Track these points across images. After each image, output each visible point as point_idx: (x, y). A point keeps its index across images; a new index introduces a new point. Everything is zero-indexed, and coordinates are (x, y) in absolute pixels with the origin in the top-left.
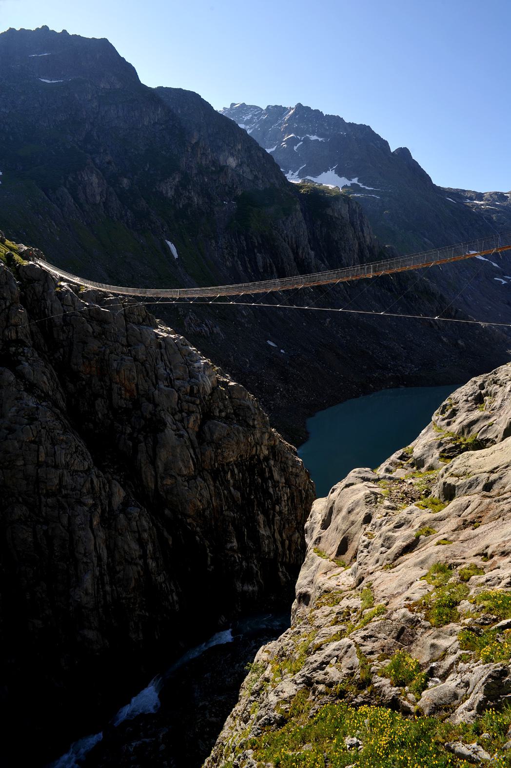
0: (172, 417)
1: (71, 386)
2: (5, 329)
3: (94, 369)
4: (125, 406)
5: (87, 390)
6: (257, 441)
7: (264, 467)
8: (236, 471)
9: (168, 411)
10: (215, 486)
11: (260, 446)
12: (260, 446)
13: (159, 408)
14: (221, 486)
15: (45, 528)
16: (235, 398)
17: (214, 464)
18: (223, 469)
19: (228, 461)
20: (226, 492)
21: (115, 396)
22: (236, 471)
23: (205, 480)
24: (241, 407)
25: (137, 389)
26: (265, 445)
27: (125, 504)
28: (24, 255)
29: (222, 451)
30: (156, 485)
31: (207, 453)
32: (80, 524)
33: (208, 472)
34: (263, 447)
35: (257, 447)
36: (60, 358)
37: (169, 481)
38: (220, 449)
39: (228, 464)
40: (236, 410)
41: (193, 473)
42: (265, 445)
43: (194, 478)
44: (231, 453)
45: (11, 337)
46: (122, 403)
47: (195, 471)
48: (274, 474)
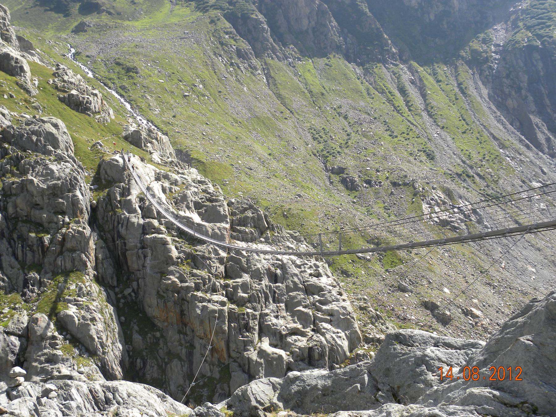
1: (137, 338)
2: (58, 256)
4: (209, 374)
28: (130, 139)
45: (65, 267)
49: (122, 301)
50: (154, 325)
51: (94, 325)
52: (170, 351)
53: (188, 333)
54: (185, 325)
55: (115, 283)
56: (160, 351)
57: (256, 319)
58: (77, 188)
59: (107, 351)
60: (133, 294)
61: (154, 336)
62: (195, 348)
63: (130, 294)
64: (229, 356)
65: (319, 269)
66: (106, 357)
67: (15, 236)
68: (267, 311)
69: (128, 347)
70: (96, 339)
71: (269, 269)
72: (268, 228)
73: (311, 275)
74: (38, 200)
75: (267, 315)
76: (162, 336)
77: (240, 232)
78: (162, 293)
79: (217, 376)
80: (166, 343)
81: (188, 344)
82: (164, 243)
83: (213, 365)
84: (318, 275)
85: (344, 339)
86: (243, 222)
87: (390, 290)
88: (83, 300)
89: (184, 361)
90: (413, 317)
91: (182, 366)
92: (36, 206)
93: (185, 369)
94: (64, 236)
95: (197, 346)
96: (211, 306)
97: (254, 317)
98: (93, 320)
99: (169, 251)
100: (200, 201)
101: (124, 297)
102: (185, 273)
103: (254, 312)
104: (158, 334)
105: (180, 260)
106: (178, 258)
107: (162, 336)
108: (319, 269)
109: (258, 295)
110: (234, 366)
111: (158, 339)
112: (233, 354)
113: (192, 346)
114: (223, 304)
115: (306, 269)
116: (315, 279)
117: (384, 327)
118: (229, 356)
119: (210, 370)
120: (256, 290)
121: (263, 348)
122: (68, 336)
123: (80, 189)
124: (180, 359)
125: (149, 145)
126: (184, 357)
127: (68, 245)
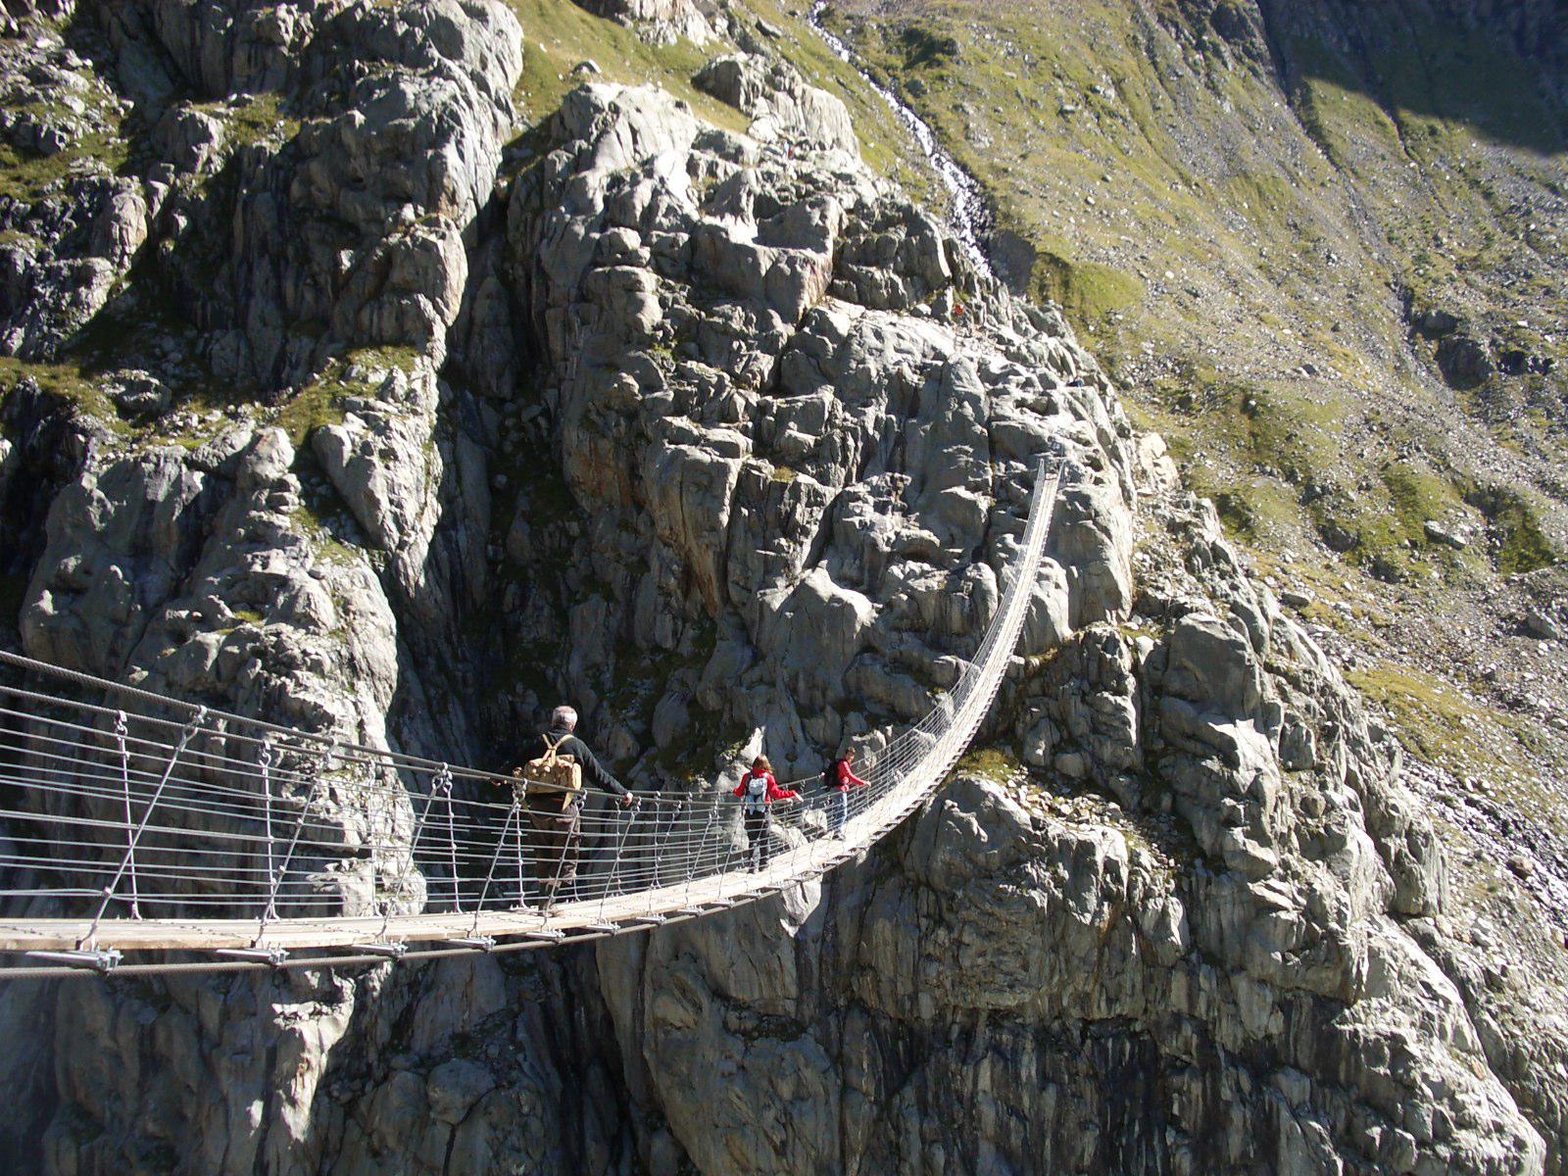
0: (795, 719)
3: (609, 474)
4: (669, 644)
5: (576, 557)
6: (1214, 944)
7: (1226, 1093)
8: (1028, 1068)
9: (793, 690)
10: (884, 1107)
11: (1225, 979)
12: (1225, 979)
13: (757, 672)
14: (924, 1113)
15: (149, 1016)
16: (1180, 696)
17: (914, 998)
18: (968, 1035)
19: (986, 1000)
20: (940, 1157)
21: (647, 597)
22: (1028, 1068)
23: (839, 1061)
24: (1190, 745)
25: (723, 573)
26: (1262, 982)
27: (463, 1043)
28: (711, 84)
29: (959, 943)
30: (639, 1013)
31: (882, 929)
32: (243, 1051)
33: (874, 1027)
34: (1242, 985)
35: (1192, 974)
36: (537, 426)
37: (674, 1011)
38: (950, 929)
39: (997, 1017)
40: (1164, 753)
41: (790, 1006)
42: (1262, 982)
43: (789, 1030)
44: (1011, 963)
45: (380, 330)
46: (664, 629)
47: (799, 1001)
48: (1284, 1154)
49: (514, 436)
50: (573, 504)
51: (387, 467)
52: (594, 572)
53: (642, 528)
54: (640, 506)
55: (507, 391)
56: (571, 572)
57: (821, 504)
58: (453, 139)
59: (411, 540)
60: (542, 422)
61: (564, 531)
62: (648, 569)
63: (533, 420)
64: (726, 599)
65: (1053, 392)
66: (405, 555)
67: (290, 251)
68: (861, 489)
69: (496, 552)
70: (385, 505)
71: (900, 375)
72: (954, 280)
73: (1021, 404)
74: (358, 166)
75: (856, 497)
76: (584, 533)
77: (855, 277)
78: (594, 416)
79: (686, 648)
80: (587, 552)
81: (634, 558)
82: (635, 285)
83: (685, 621)
84: (1047, 409)
85: (1057, 586)
86: (876, 254)
87: (1500, 628)
88: (390, 408)
89: (618, 602)
90: (1542, 702)
91: (609, 613)
92: (355, 183)
93: (613, 622)
94: (390, 251)
95: (655, 564)
96: (695, 453)
97: (815, 499)
98: (389, 455)
99: (640, 305)
100: (775, 195)
101: (521, 429)
102: (662, 367)
103: (818, 486)
104: (574, 528)
105: (660, 334)
106: (655, 328)
107: (584, 533)
108: (1053, 392)
109: (844, 440)
110: (726, 627)
111: (572, 540)
112: (735, 594)
113: (644, 564)
114: (729, 450)
115: (1012, 387)
116: (1030, 419)
117: (1224, 586)
118: (726, 599)
119: (675, 633)
120: (844, 429)
121: (809, 582)
122: (322, 490)
123: (459, 143)
124: (609, 597)
125: (761, 102)
126: (618, 593)
127: (396, 276)
